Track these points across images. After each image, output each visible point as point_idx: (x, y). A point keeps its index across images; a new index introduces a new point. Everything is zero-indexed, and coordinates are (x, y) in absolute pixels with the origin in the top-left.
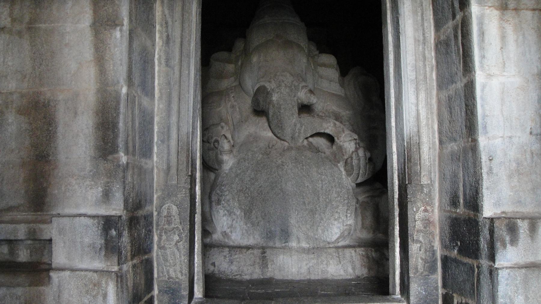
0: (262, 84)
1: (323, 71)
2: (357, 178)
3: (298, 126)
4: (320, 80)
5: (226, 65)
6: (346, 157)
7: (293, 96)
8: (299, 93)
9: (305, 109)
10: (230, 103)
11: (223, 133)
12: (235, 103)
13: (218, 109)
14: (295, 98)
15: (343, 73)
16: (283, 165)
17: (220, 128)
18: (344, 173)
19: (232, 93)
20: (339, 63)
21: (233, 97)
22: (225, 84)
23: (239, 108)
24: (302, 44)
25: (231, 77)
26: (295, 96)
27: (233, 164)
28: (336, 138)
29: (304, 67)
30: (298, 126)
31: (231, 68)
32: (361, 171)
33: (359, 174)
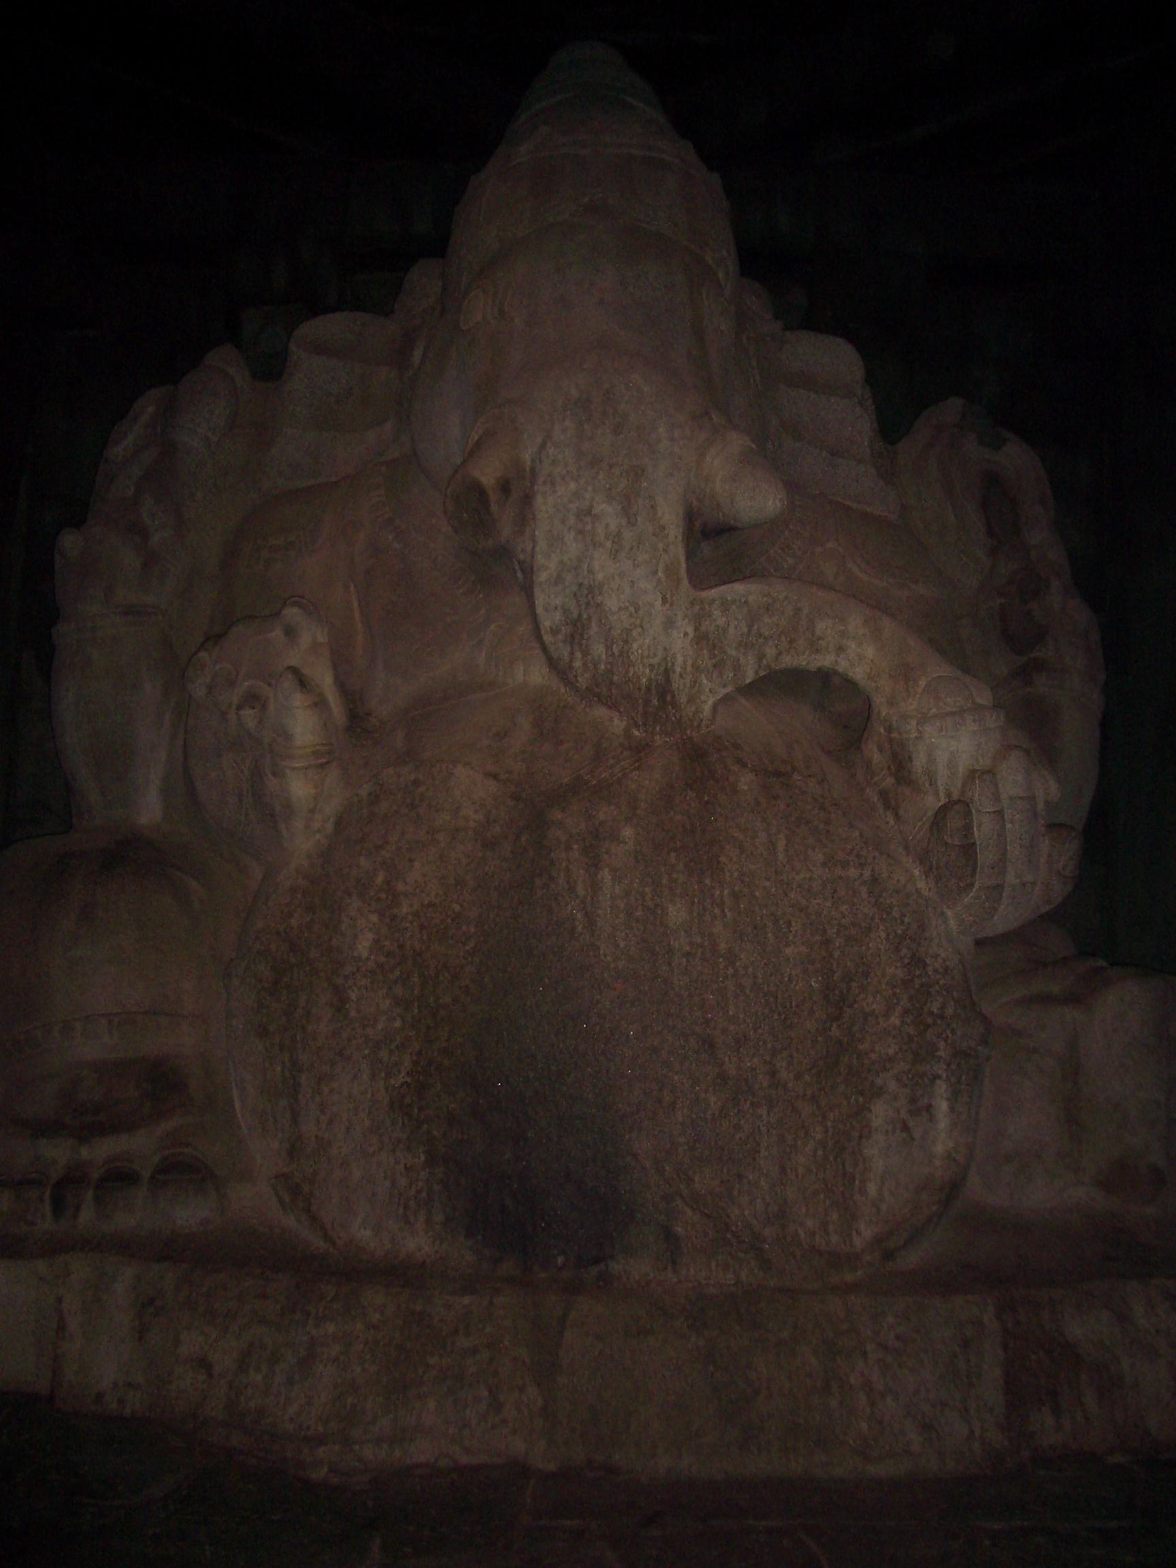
11: (294, 662)
15: (892, 426)
17: (277, 634)
20: (870, 379)
33: (999, 888)
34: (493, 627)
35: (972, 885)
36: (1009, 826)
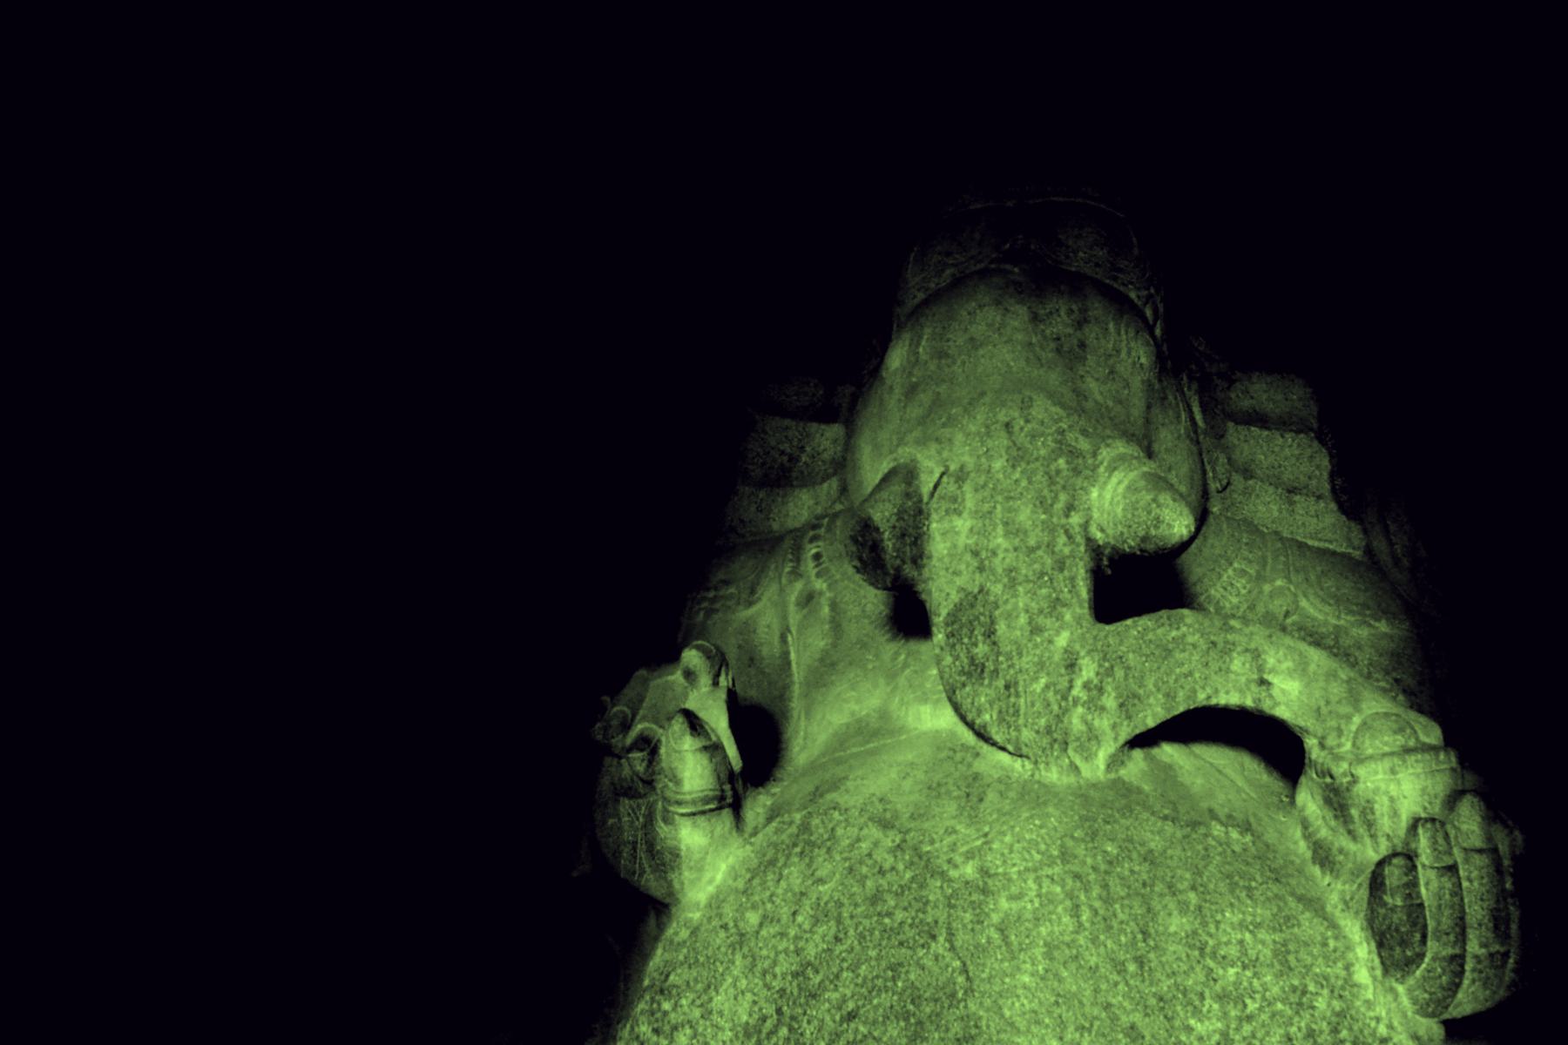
0: (905, 453)
1: (1251, 445)
2: (1455, 987)
3: (1088, 670)
4: (1237, 480)
5: (813, 427)
6: (1371, 854)
7: (1059, 506)
8: (1095, 494)
9: (1135, 583)
10: (799, 586)
11: (690, 705)
12: (820, 585)
13: (745, 614)
14: (1076, 519)
16: (985, 891)
17: (677, 677)
18: (1363, 952)
19: (814, 539)
21: (817, 557)
22: (801, 506)
23: (834, 606)
24: (1133, 295)
25: (824, 480)
26: (1070, 508)
27: (734, 874)
28: (1311, 743)
29: (1137, 382)
30: (1088, 670)
31: (827, 438)
32: (1473, 947)
33: (1458, 960)
34: (907, 671)
35: (1421, 956)
36: (1465, 884)
